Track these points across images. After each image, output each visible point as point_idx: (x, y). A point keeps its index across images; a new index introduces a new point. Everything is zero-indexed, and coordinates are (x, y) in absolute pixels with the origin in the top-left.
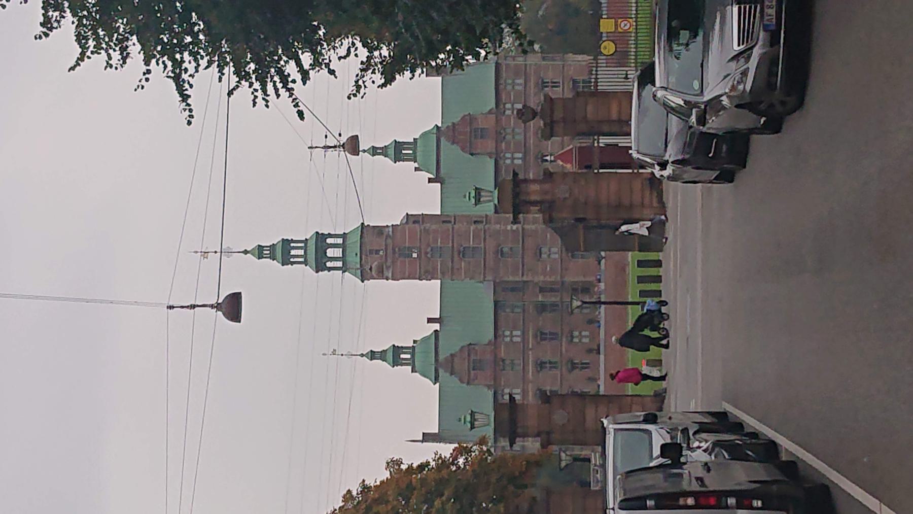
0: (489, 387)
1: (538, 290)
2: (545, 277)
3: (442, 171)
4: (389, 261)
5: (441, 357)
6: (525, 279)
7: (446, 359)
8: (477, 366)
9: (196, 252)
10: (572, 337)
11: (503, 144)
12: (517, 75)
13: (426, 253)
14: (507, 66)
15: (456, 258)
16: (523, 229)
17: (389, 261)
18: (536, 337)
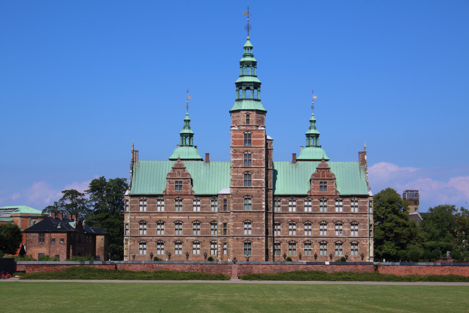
0: (165, 191)
1: (225, 221)
2: (232, 226)
3: (300, 162)
4: (242, 128)
5: (184, 162)
6: (232, 213)
7: (183, 165)
8: (179, 185)
9: (248, 8)
10: (197, 244)
11: (317, 200)
12: (360, 209)
13: (247, 151)
14: (366, 203)
15: (243, 170)
16: (263, 212)
17: (242, 128)
18: (197, 221)
